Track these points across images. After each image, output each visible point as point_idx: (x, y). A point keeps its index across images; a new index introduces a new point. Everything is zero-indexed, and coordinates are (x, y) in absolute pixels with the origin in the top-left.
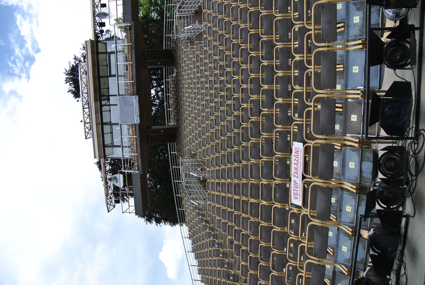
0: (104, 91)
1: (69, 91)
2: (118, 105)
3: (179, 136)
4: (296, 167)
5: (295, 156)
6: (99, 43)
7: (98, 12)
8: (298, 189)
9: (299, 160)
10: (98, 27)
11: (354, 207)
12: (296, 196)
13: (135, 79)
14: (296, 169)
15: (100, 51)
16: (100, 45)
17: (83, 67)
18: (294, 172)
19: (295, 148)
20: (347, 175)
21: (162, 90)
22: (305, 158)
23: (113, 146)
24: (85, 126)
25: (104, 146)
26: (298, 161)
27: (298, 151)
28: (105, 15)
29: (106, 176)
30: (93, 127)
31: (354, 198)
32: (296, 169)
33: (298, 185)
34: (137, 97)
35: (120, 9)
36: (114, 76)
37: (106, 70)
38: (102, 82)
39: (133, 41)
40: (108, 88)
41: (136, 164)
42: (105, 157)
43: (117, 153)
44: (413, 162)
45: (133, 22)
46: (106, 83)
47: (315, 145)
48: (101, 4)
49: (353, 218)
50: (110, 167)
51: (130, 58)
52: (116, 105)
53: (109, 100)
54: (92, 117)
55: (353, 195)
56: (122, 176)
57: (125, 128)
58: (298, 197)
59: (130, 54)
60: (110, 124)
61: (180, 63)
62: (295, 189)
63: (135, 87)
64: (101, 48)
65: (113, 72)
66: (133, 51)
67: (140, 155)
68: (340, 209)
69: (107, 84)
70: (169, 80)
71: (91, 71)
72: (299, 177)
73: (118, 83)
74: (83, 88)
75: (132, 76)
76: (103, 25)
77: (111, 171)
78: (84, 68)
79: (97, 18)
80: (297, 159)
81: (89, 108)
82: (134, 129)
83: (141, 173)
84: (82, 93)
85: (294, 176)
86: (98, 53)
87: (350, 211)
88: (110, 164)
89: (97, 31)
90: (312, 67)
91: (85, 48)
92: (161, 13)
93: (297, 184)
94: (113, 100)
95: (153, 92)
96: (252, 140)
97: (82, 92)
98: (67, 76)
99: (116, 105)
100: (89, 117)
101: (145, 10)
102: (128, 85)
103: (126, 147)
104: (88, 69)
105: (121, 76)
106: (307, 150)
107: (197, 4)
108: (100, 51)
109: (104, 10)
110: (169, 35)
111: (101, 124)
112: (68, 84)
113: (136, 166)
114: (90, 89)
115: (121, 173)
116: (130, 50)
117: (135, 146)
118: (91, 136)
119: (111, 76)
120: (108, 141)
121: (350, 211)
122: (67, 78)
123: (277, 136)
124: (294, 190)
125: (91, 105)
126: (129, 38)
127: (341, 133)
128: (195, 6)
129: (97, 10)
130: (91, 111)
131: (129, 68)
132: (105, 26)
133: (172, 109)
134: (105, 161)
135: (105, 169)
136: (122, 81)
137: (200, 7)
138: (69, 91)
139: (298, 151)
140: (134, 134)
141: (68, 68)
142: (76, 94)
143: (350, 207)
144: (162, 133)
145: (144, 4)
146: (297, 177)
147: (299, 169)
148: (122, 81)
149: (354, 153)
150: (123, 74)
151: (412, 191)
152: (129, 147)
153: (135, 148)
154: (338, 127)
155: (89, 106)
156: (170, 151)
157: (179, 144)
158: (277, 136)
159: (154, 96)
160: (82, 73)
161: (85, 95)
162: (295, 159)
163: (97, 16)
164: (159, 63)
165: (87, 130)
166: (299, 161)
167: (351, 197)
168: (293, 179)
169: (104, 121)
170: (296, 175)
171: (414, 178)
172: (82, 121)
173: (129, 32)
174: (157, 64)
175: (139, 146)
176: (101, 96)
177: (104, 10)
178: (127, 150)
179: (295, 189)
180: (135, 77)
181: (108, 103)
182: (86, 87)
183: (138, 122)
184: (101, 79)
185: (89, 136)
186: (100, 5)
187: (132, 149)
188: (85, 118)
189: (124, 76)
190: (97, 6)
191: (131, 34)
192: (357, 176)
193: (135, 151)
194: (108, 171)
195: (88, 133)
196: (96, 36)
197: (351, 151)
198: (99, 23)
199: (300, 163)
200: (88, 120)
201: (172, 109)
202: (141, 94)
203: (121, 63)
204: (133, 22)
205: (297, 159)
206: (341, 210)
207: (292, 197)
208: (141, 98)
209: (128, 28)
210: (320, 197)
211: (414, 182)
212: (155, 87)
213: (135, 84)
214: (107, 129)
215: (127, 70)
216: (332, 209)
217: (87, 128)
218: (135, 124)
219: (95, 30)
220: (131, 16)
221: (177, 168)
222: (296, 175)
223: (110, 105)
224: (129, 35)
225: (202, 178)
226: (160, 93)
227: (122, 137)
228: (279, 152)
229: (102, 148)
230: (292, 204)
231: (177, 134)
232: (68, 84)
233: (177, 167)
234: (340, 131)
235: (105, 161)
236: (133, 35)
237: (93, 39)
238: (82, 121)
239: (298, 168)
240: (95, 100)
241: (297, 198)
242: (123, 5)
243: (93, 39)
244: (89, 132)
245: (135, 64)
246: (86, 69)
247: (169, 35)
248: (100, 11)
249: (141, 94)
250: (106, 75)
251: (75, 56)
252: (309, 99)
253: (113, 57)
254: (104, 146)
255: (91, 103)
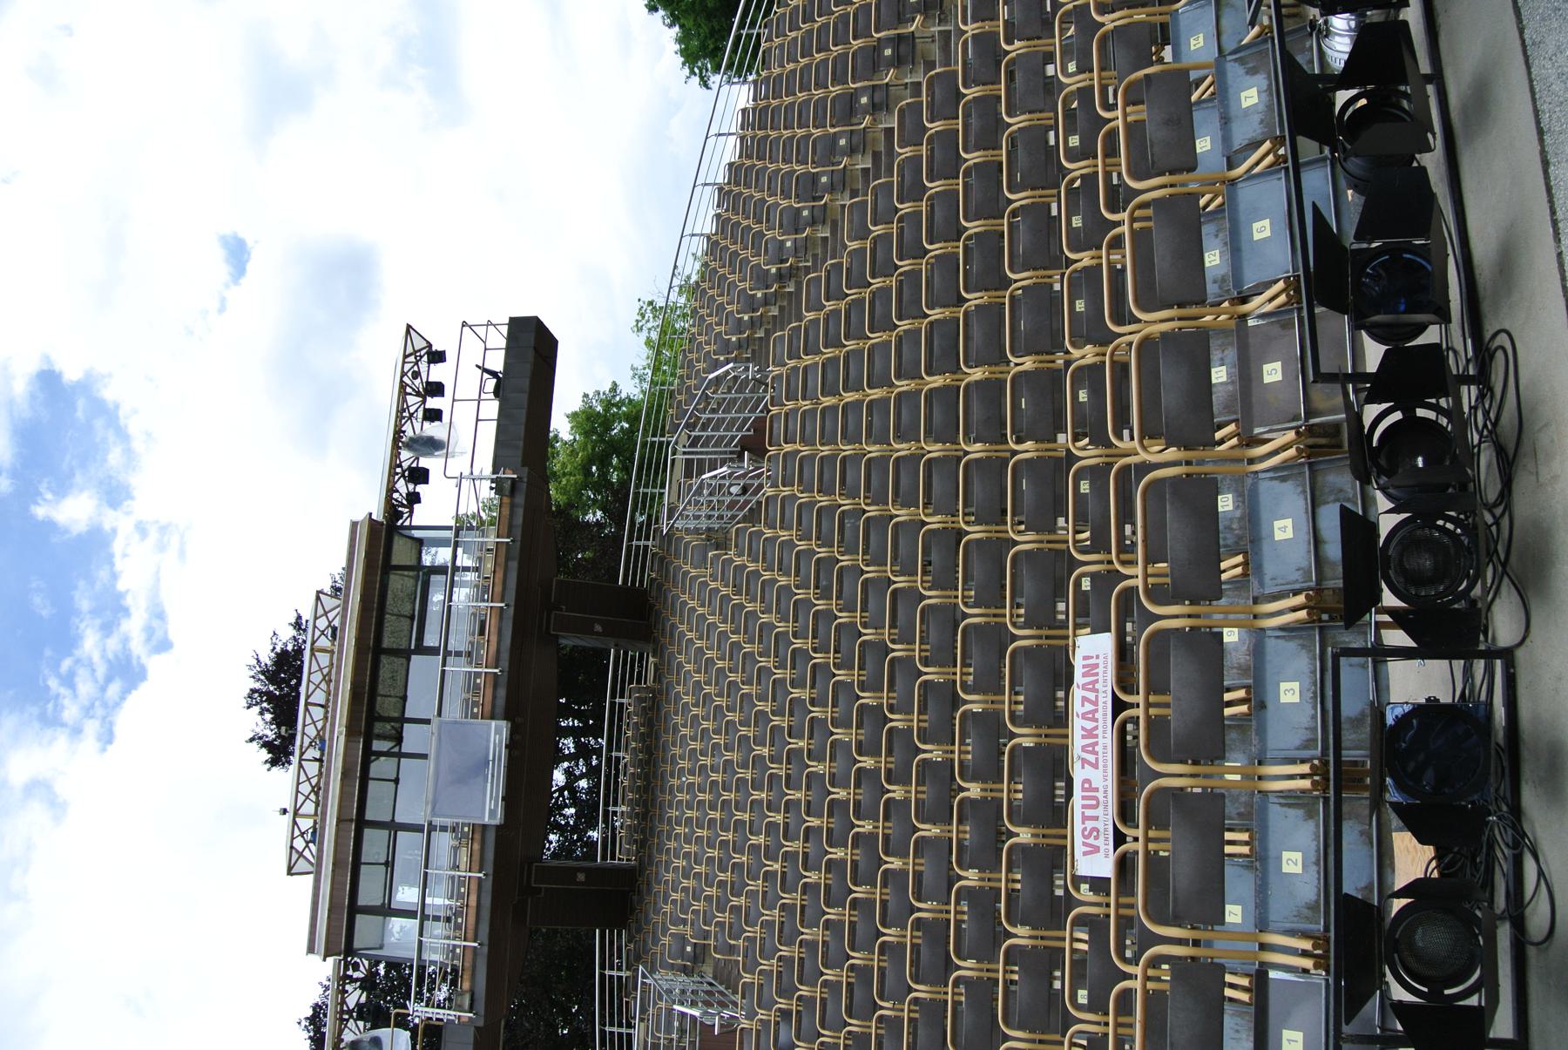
0: (386, 706)
1: (252, 740)
2: (432, 756)
3: (641, 901)
4: (1089, 725)
5: (1084, 687)
6: (396, 538)
7: (410, 433)
8: (1099, 812)
9: (1101, 695)
10: (401, 485)
11: (1308, 681)
12: (1091, 841)
13: (505, 663)
14: (1090, 734)
15: (395, 561)
16: (399, 545)
17: (326, 613)
18: (1084, 749)
19: (1085, 658)
20: (1270, 569)
21: (593, 773)
22: (1122, 732)
23: (387, 910)
24: (295, 823)
25: (354, 909)
26: (1095, 703)
27: (1097, 666)
28: (432, 445)
29: (341, 1032)
30: (323, 828)
31: (1303, 646)
32: (1090, 734)
33: (1100, 795)
34: (504, 726)
35: (489, 432)
36: (433, 651)
37: (406, 633)
38: (384, 673)
39: (518, 532)
40: (404, 698)
41: (466, 985)
42: (349, 950)
43: (400, 935)
44: (1489, 466)
45: (526, 469)
46: (400, 678)
47: (1150, 580)
48: (426, 410)
49: (1312, 725)
50: (363, 999)
51: (498, 589)
52: (424, 756)
53: (399, 739)
54: (326, 798)
55: (1301, 637)
56: (404, 1036)
57: (444, 842)
58: (1100, 843)
59: (500, 575)
60: (393, 827)
61: (673, 625)
62: (1089, 812)
63: (502, 692)
64: (401, 553)
65: (431, 640)
66: (514, 565)
67: (486, 949)
68: (1251, 539)
69: (400, 683)
70: (624, 701)
71: (354, 624)
72: (1101, 764)
73: (443, 672)
74: (312, 687)
75: (498, 651)
76: (420, 476)
77: (362, 1012)
78: (331, 616)
79: (405, 455)
80: (1091, 696)
81: (320, 760)
82: (476, 846)
83: (481, 1023)
84: (307, 704)
85: (1084, 761)
86: (388, 568)
87: (1296, 699)
88: (368, 983)
89: (396, 495)
90: (1138, 570)
91: (339, 589)
92: (616, 514)
93: (1097, 790)
94: (413, 738)
95: (559, 777)
96: (925, 751)
97: (308, 697)
98: (257, 685)
99: (424, 756)
100: (317, 794)
101: (564, 491)
102: (477, 687)
103: (436, 918)
104: (343, 623)
105: (458, 654)
106: (1124, 653)
107: (753, 411)
108: (395, 561)
109: (432, 430)
110: (642, 543)
111: (357, 822)
112: (256, 709)
113: (462, 994)
114: (336, 695)
115: (402, 1022)
116: (502, 560)
117: (472, 912)
118: (311, 869)
119: (422, 650)
120: (370, 893)
121: (1296, 699)
122: (253, 691)
123: (1016, 703)
124: (1085, 818)
125: (331, 747)
126: (505, 521)
127: (1241, 519)
128: (746, 420)
129: (407, 428)
130: (328, 775)
131: (492, 624)
132: (426, 482)
133: (624, 808)
134: (346, 969)
135: (343, 1002)
136: (458, 669)
137: (759, 425)
138: (252, 740)
139: (1097, 666)
140: (476, 866)
141: (267, 658)
142: (279, 752)
143: (1296, 685)
144: (581, 883)
145: (564, 474)
146: (1095, 766)
147: (1099, 732)
148: (458, 669)
149: (1288, 487)
150: (463, 648)
151: (1502, 557)
152: (448, 920)
153: (472, 920)
154: (1230, 502)
155: (322, 750)
156: (602, 967)
157: (639, 930)
158: (1016, 703)
159: (561, 790)
160: (317, 633)
161: (318, 713)
162: (1084, 699)
163: (408, 446)
164: (598, 628)
165: (299, 844)
166: (1101, 700)
167: (1292, 645)
168: (1079, 774)
169: (369, 816)
170: (1091, 758)
171: (1498, 511)
172: (285, 811)
173: (506, 500)
174: (589, 631)
175: (486, 914)
176: (375, 719)
177: (432, 430)
178: (438, 929)
179: (1089, 812)
180: (505, 656)
181: (396, 750)
182: (324, 685)
183: (498, 819)
184: (384, 659)
185: (302, 865)
186: (420, 414)
187: (458, 927)
188: (301, 798)
189: (469, 654)
190: (411, 415)
191: (513, 506)
192: (1304, 564)
193: (471, 934)
194: (350, 1012)
195: (301, 854)
196: (392, 511)
197: (1276, 483)
198: (410, 468)
199: (1105, 708)
200: (309, 808)
201: (624, 808)
202: (519, 720)
203: (463, 602)
204: (526, 469)
205: (1091, 696)
206: (1262, 706)
207: (1079, 849)
208: (518, 737)
209: (507, 485)
210: (1180, 669)
211: (1505, 522)
212: (569, 758)
213: (504, 681)
214: (375, 843)
215: (482, 633)
216: (1230, 809)
217: (302, 834)
218: (484, 827)
219: (391, 490)
220: (520, 453)
221: (621, 1035)
222: (1091, 758)
223: (400, 755)
224: (506, 511)
225: (721, 1026)
226: (583, 783)
227: (426, 874)
228: (1020, 1028)
229: (343, 923)
230: (1078, 880)
231: (635, 898)
232: (256, 709)
233: (624, 1030)
234: (1238, 514)
235: (346, 969)
236: (520, 512)
237: (378, 516)
238: (285, 811)
239: (1096, 728)
240: (351, 732)
241: (1096, 849)
242: (498, 420)
243: (378, 516)
244: (307, 853)
245: (512, 610)
246: (336, 623)
247: (642, 543)
248: (418, 431)
249: (519, 720)
250: (404, 646)
251: (299, 617)
252: (1126, 433)
253: (438, 584)
254: (354, 909)
255: (331, 739)
